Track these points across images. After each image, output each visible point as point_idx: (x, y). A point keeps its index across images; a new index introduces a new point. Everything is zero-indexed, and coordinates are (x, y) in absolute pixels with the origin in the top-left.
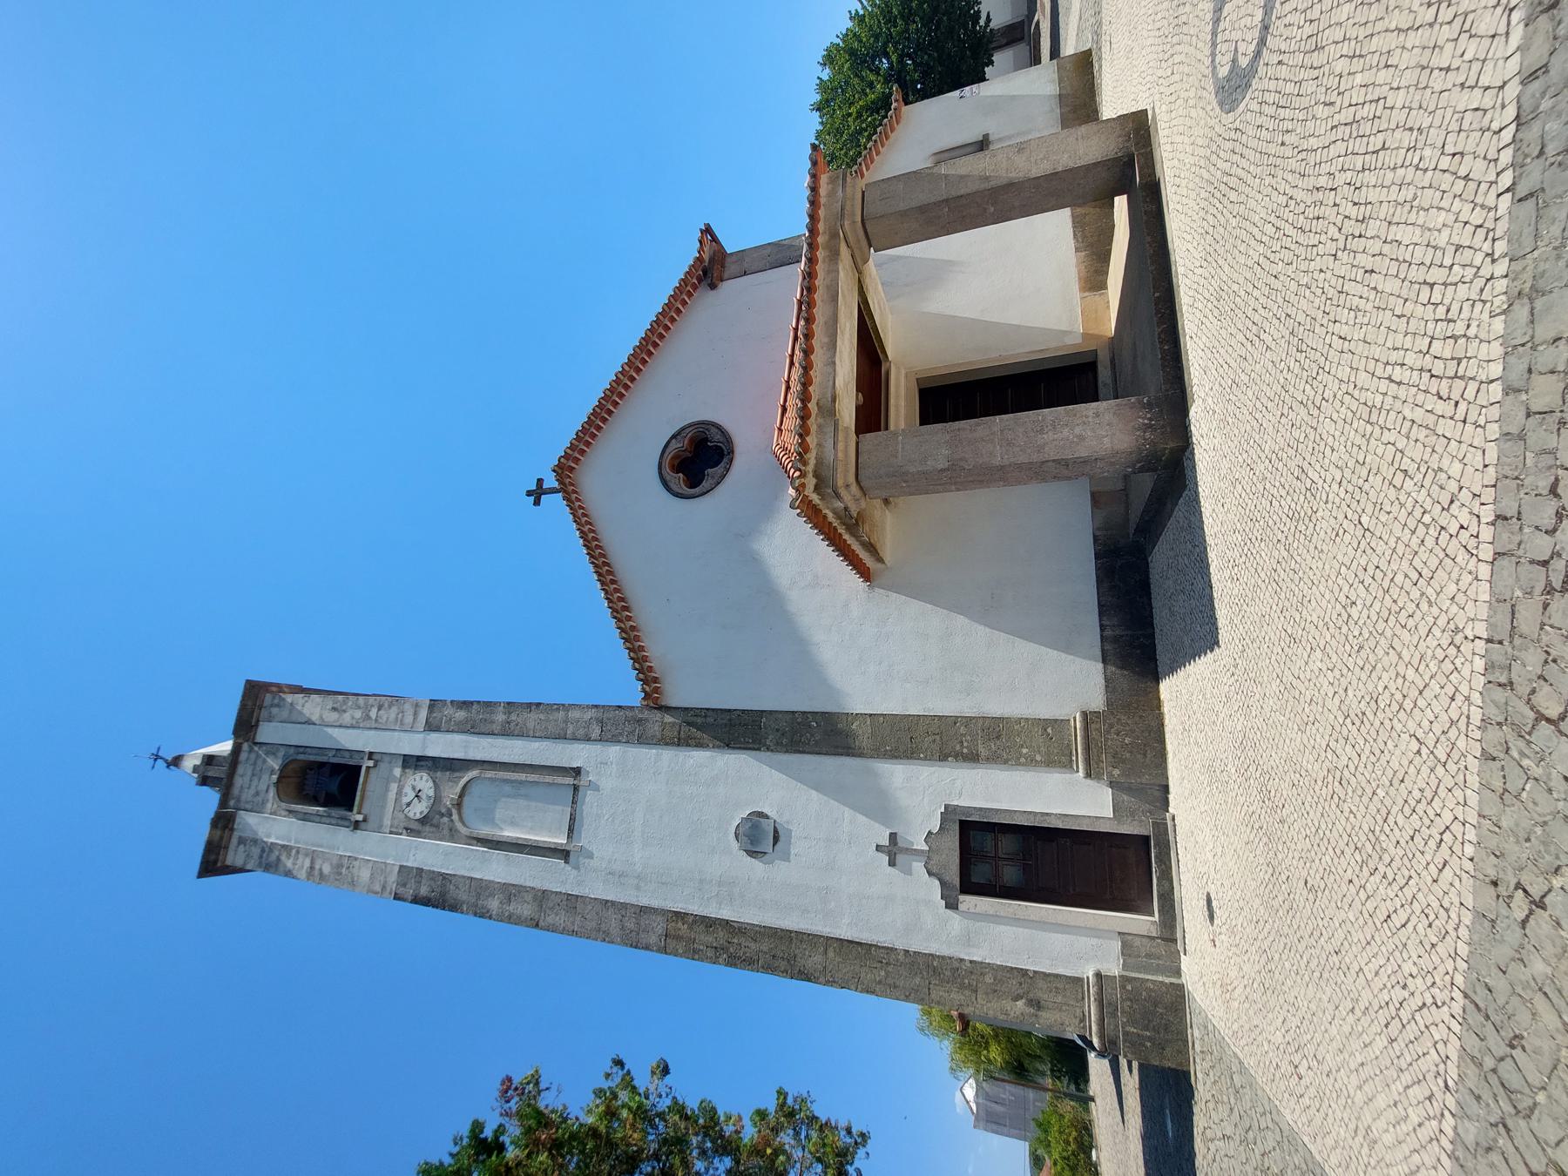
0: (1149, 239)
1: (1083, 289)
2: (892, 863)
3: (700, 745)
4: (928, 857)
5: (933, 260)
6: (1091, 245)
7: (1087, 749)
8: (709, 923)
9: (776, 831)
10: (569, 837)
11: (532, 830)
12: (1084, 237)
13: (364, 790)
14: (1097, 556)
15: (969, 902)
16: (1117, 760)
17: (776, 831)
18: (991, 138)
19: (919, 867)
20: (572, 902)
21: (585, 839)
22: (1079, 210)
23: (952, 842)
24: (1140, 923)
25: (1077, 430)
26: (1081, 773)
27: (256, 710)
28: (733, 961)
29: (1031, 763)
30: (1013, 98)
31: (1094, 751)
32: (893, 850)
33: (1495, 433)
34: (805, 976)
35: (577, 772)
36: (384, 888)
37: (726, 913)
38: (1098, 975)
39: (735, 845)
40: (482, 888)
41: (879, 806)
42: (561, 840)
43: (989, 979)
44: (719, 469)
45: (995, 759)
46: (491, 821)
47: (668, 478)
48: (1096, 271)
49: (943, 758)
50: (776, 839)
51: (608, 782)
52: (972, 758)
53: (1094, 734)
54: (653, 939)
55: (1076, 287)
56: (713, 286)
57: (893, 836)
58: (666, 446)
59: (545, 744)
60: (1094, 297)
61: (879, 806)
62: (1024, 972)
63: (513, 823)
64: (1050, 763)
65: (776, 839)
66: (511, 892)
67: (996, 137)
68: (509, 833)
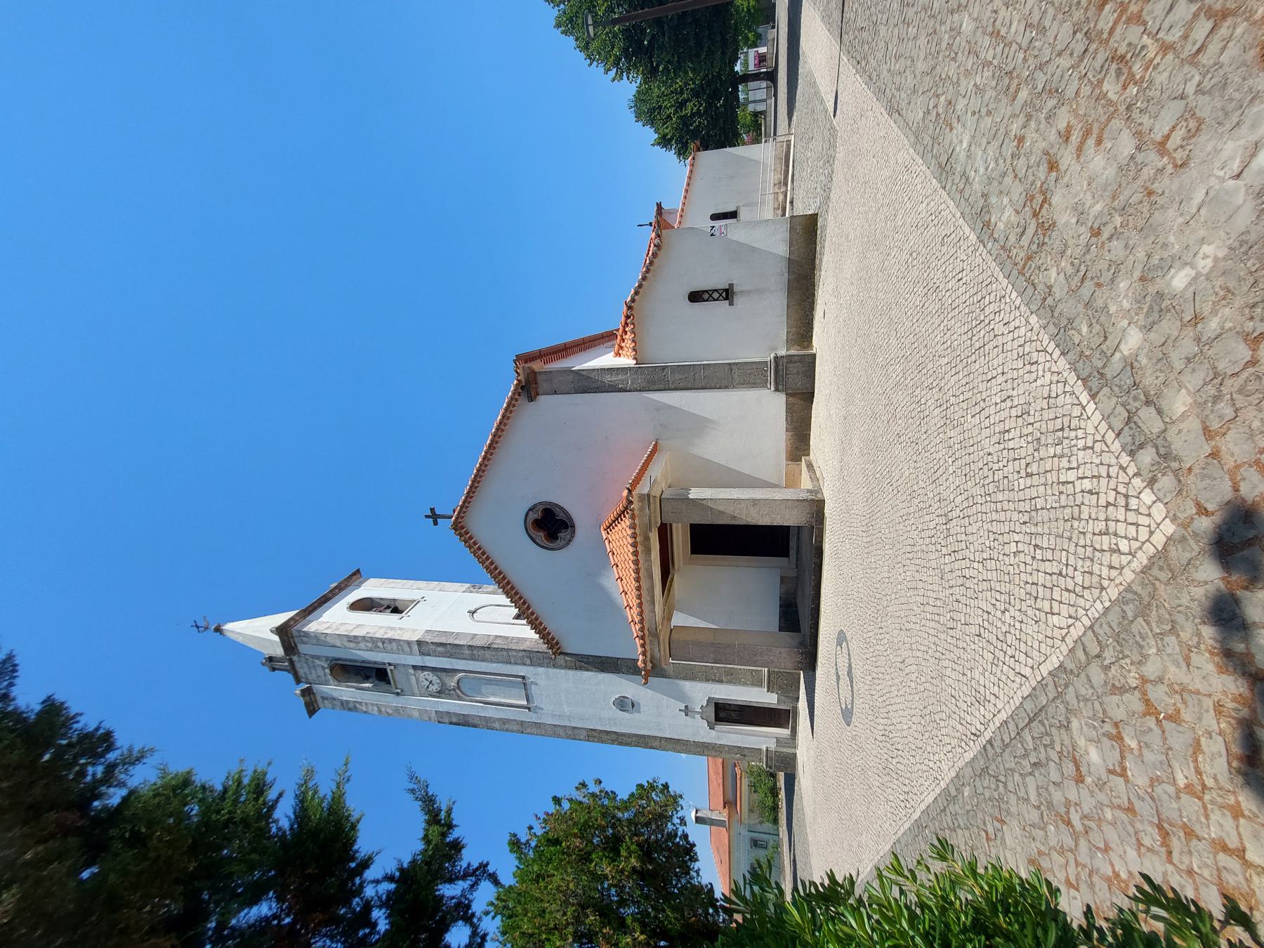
0: (813, 577)
1: (788, 459)
2: (686, 715)
3: (587, 670)
4: (701, 714)
5: (694, 414)
6: (795, 428)
7: (769, 683)
8: (607, 733)
9: (632, 703)
10: (528, 700)
11: (505, 697)
12: (792, 421)
13: (393, 679)
14: (781, 606)
15: (718, 727)
16: (780, 688)
17: (632, 703)
18: (736, 289)
19: (698, 716)
20: (538, 725)
21: (536, 703)
22: (791, 399)
23: (712, 709)
24: (784, 732)
25: (771, 658)
26: (766, 689)
27: (291, 640)
28: (620, 744)
29: (745, 684)
30: (754, 249)
31: (772, 684)
32: (687, 711)
33: (1073, 378)
34: (651, 748)
35: (523, 677)
36: (430, 719)
37: (614, 729)
38: (767, 748)
39: (614, 708)
40: (487, 719)
41: (680, 696)
42: (525, 703)
43: (726, 749)
44: (557, 511)
45: (729, 682)
46: (482, 695)
47: (534, 536)
48: (797, 448)
49: (707, 680)
50: (633, 706)
51: (542, 682)
52: (721, 681)
53: (772, 678)
54: (582, 737)
55: (784, 456)
56: (531, 399)
57: (686, 707)
58: (543, 547)
59: (499, 665)
60: (793, 465)
61: (680, 696)
62: (740, 747)
63: (493, 695)
64: (753, 685)
65: (633, 706)
66: (504, 721)
67: (741, 288)
68: (492, 699)
